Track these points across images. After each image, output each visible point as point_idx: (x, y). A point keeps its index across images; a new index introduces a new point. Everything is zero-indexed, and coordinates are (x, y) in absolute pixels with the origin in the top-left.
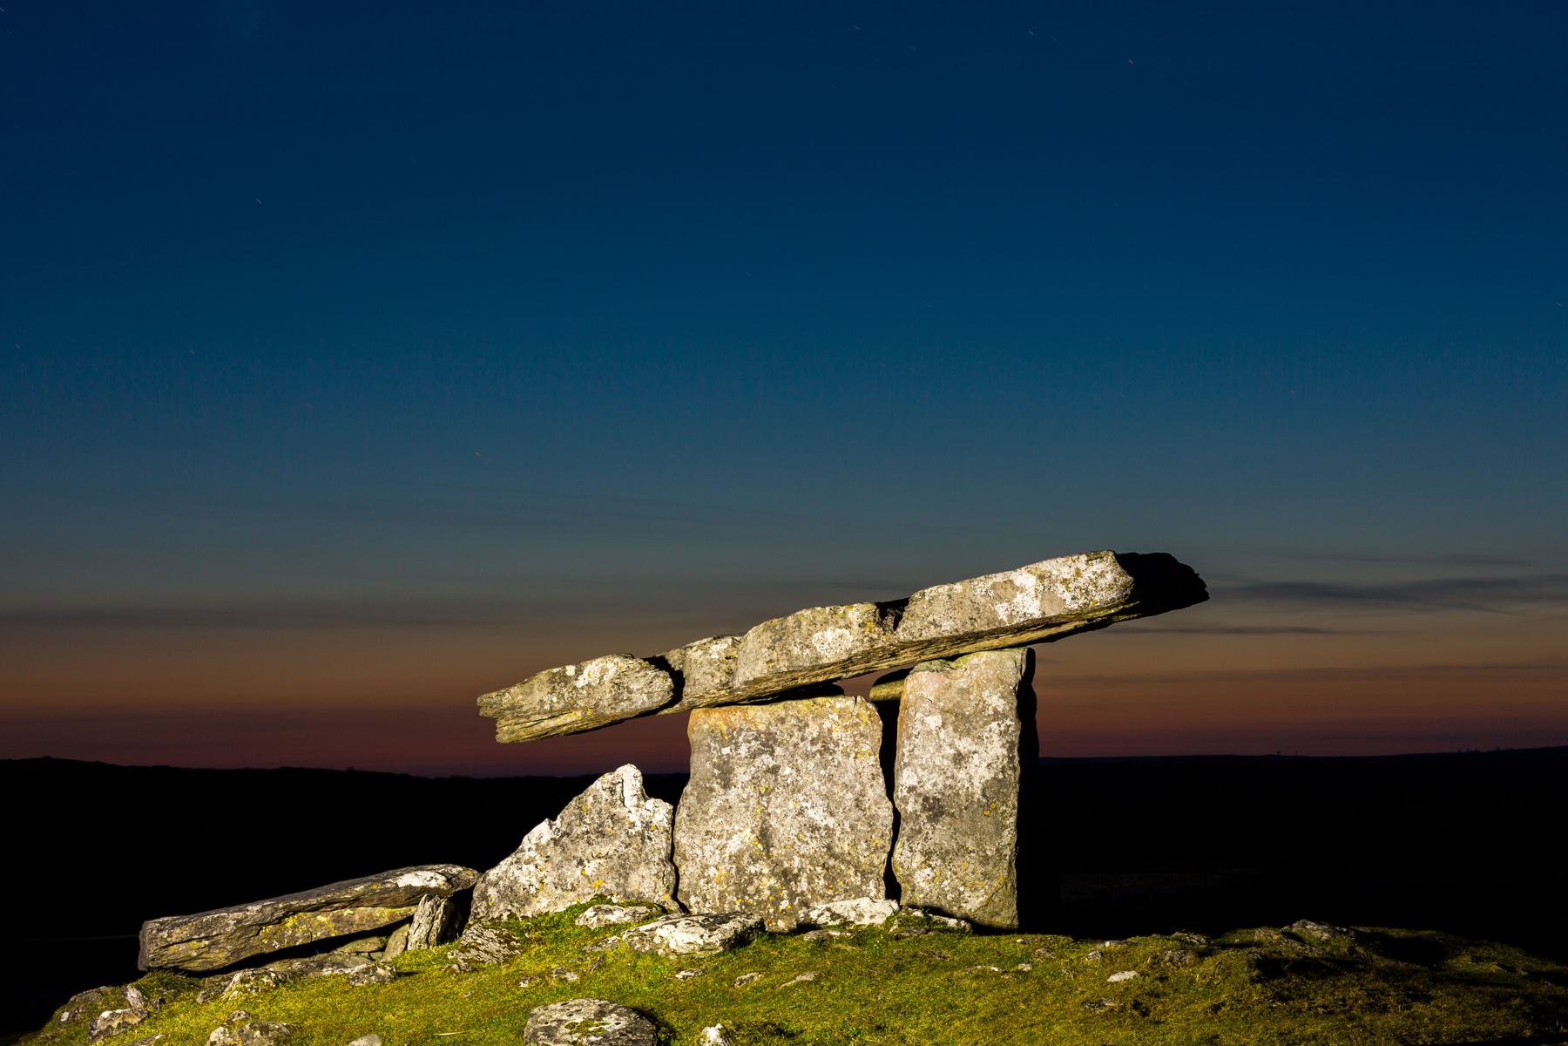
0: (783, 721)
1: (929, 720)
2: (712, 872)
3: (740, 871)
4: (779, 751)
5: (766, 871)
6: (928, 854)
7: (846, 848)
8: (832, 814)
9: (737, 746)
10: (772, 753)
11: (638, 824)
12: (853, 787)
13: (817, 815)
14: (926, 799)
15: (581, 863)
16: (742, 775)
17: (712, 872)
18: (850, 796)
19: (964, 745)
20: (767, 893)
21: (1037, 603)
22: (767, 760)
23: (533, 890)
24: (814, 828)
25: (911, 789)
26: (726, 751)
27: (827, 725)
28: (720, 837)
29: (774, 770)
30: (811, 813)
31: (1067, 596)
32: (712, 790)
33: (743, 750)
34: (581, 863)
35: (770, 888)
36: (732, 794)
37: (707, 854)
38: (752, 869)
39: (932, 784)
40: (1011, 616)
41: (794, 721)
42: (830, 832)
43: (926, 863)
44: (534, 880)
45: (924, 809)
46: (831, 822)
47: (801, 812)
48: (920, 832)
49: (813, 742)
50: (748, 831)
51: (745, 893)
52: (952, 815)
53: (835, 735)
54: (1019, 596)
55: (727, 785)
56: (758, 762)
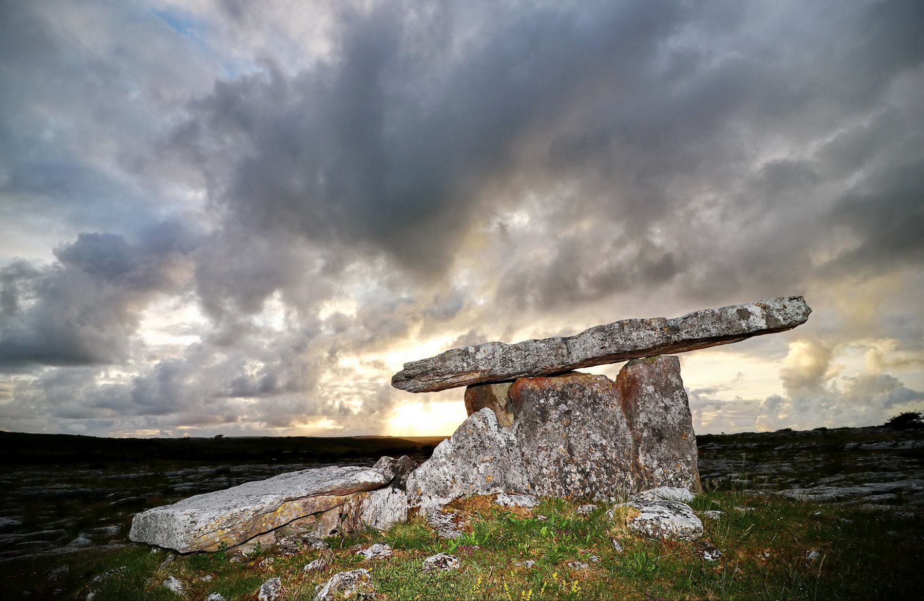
0: (571, 386)
1: (648, 388)
2: (544, 471)
3: (561, 469)
4: (570, 402)
5: (574, 470)
6: (660, 460)
7: (614, 457)
8: (605, 438)
9: (547, 399)
10: (566, 404)
11: (503, 442)
12: (613, 423)
13: (596, 437)
14: (654, 430)
15: (475, 465)
16: (554, 415)
17: (544, 471)
18: (612, 427)
19: (667, 401)
20: (578, 483)
21: (764, 321)
22: (563, 407)
23: (449, 483)
24: (596, 445)
25: (645, 424)
26: (542, 401)
27: (595, 389)
28: (547, 450)
29: (568, 413)
30: (593, 436)
31: (780, 318)
32: (537, 423)
33: (551, 401)
34: (475, 465)
35: (579, 480)
36: (549, 426)
37: (541, 460)
38: (566, 469)
39: (657, 421)
40: (749, 328)
41: (577, 386)
42: (603, 448)
43: (659, 466)
44: (448, 477)
45: (654, 436)
46: (604, 442)
47: (588, 436)
48: (653, 447)
49: (589, 398)
50: (562, 447)
51: (565, 482)
52: (667, 439)
53: (599, 395)
54: (752, 317)
55: (544, 420)
56: (560, 407)
